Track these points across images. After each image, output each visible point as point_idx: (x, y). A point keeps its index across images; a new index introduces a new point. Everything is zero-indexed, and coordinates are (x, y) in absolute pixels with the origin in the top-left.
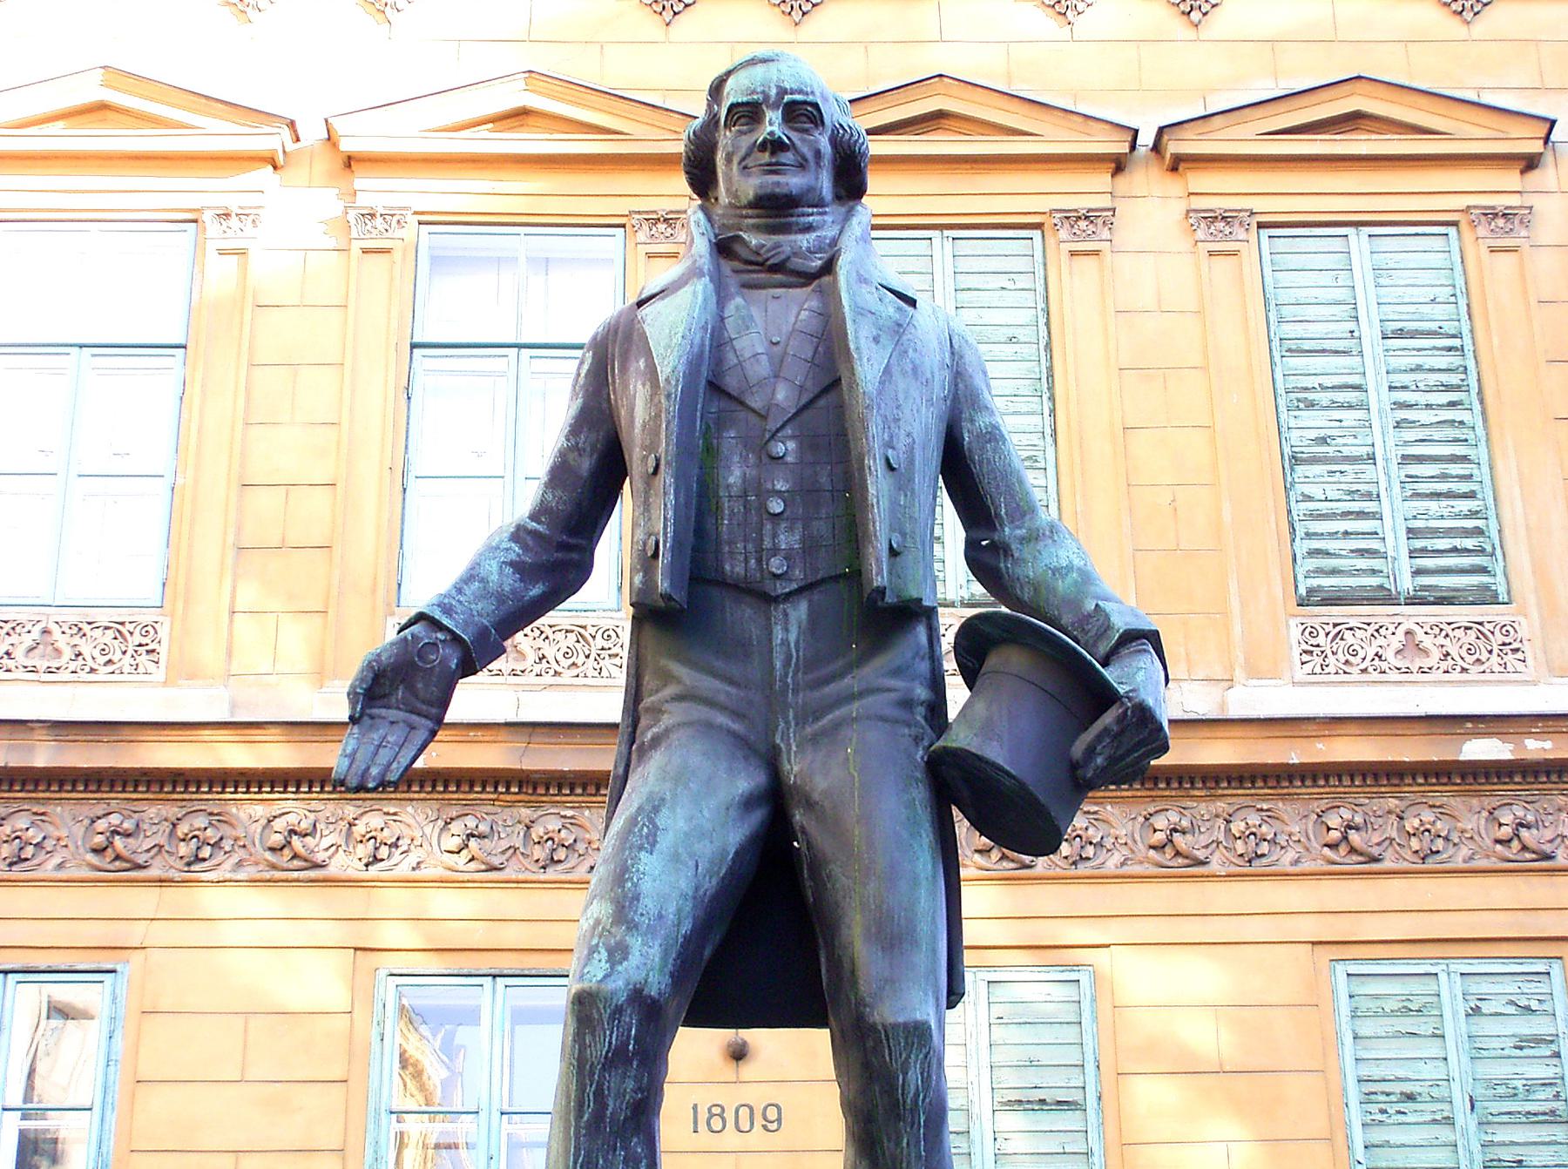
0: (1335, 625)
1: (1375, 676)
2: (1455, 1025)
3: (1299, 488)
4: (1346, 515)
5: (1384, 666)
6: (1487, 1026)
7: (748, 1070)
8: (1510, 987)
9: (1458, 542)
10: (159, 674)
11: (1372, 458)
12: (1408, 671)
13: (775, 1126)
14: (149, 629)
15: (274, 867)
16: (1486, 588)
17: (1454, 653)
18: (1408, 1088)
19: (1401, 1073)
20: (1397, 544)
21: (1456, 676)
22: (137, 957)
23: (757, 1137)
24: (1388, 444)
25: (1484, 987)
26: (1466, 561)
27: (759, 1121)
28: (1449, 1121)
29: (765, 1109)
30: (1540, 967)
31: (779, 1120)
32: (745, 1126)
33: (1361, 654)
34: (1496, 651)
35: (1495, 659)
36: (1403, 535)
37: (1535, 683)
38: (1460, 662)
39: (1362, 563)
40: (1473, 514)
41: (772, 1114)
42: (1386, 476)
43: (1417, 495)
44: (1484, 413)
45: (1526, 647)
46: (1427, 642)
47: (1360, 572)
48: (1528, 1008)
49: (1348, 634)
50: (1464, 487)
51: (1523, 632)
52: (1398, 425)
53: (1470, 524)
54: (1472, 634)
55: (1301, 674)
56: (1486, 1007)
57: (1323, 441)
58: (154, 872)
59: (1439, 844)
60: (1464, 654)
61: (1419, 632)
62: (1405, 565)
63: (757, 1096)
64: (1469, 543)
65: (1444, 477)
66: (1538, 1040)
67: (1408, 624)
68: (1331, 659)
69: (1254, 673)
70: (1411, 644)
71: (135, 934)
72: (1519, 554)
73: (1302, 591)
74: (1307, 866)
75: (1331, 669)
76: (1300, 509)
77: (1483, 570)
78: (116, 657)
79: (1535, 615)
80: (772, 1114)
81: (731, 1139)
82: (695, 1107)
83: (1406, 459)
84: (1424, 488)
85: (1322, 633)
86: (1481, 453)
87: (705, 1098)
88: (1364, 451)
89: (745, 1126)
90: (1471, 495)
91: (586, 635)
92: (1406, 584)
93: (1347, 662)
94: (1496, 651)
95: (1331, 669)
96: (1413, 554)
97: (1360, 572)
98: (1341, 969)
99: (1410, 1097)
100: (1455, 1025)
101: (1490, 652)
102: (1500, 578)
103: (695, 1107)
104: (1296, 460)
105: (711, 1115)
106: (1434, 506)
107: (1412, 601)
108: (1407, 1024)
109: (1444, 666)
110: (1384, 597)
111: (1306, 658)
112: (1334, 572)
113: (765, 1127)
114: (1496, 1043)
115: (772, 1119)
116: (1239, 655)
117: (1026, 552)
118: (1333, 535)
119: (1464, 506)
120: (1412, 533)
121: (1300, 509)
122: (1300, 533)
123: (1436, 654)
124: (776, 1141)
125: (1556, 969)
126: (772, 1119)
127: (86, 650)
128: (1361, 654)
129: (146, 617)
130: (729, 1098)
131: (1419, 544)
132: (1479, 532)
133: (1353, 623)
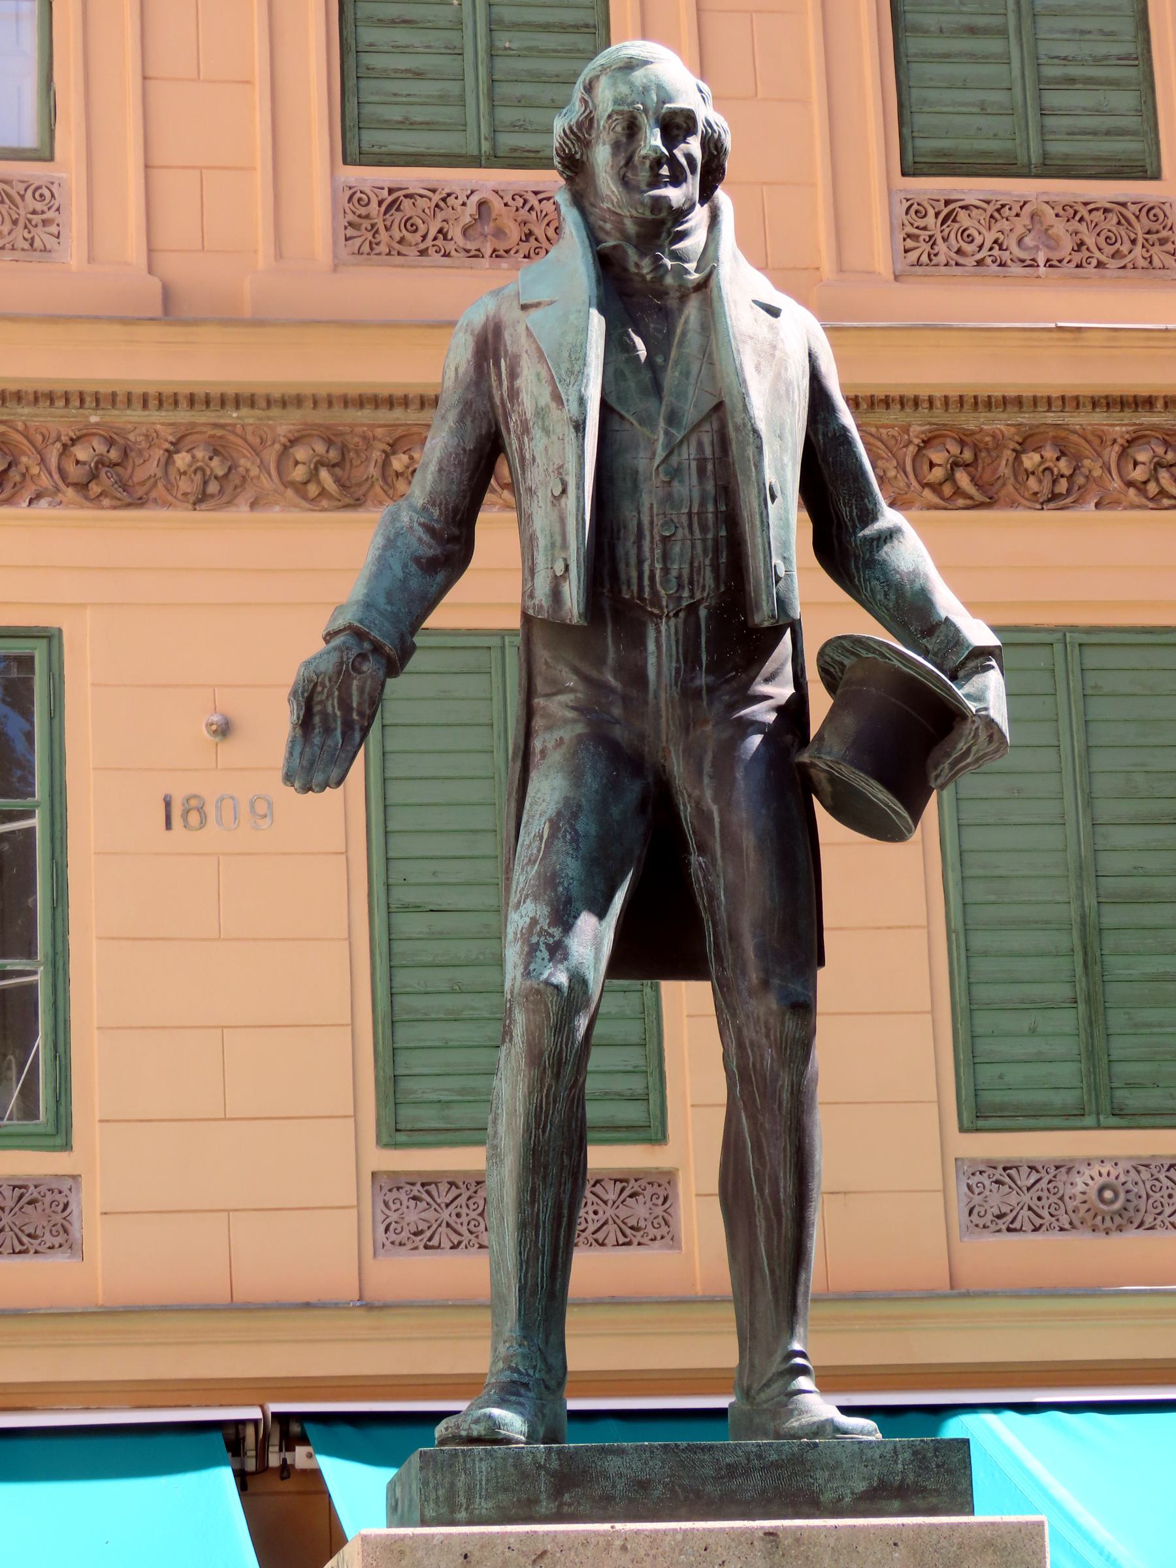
0: (947, 203)
5: (1006, 256)
17: (1090, 241)
21: (1090, 270)
33: (978, 240)
34: (1140, 241)
35: (1138, 250)
38: (1097, 254)
49: (963, 214)
60: (1103, 244)
75: (942, 259)
85: (931, 212)
91: (13, 193)
93: (959, 252)
94: (1140, 241)
95: (942, 259)
101: (1134, 242)
109: (1077, 257)
111: (910, 243)
128: (978, 240)
133: (970, 200)
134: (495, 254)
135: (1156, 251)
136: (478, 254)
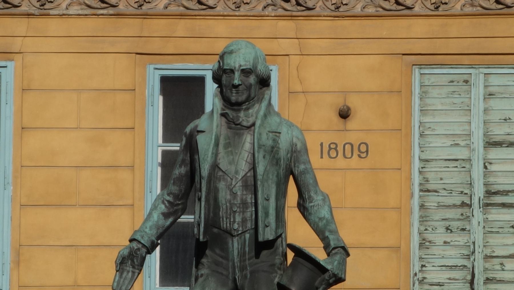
7: (352, 124)
13: (364, 155)
23: (355, 161)
27: (356, 152)
29: (360, 145)
31: (367, 151)
32: (348, 154)
41: (363, 148)
63: (354, 138)
80: (363, 148)
81: (341, 162)
82: (322, 145)
87: (327, 139)
89: (348, 154)
103: (322, 145)
105: (330, 149)
113: (359, 156)
115: (363, 151)
124: (365, 163)
126: (363, 151)
130: (340, 140)
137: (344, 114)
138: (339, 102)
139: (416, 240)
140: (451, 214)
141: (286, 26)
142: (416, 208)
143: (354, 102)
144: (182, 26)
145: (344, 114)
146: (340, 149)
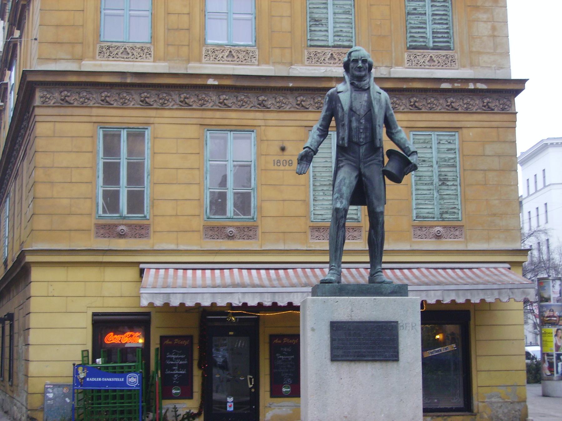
1: (423, 67)
2: (435, 146)
3: (409, 21)
4: (419, 28)
6: (442, 146)
7: (285, 153)
8: (447, 138)
9: (443, 35)
10: (152, 59)
11: (425, 14)
12: (430, 66)
14: (149, 48)
15: (181, 106)
16: (449, 46)
18: (424, 159)
19: (423, 156)
20: (429, 35)
21: (440, 67)
22: (152, 126)
24: (429, 10)
25: (441, 138)
26: (445, 40)
27: (288, 164)
28: (432, 166)
30: (453, 134)
35: (449, 63)
36: (431, 33)
37: (457, 69)
39: (421, 40)
40: (447, 28)
41: (290, 162)
42: (428, 18)
43: (435, 23)
44: (451, 3)
45: (456, 61)
46: (435, 59)
47: (420, 42)
48: (450, 143)
50: (445, 22)
51: (456, 57)
52: (432, 6)
53: (446, 31)
54: (445, 58)
55: (407, 65)
56: (442, 142)
57: (415, 9)
58: (155, 106)
59: (434, 106)
61: (433, 57)
62: (431, 40)
63: (287, 158)
64: (446, 35)
65: (441, 19)
66: (451, 149)
67: (431, 55)
68: (414, 63)
69: (397, 65)
70: (431, 60)
71: (152, 120)
72: (457, 39)
73: (408, 46)
74: (405, 110)
76: (409, 26)
77: (448, 42)
78: (142, 55)
79: (459, 52)
80: (290, 162)
81: (282, 167)
83: (433, 15)
84: (437, 21)
86: (450, 14)
87: (276, 158)
88: (424, 12)
90: (447, 24)
92: (431, 45)
96: (433, 37)
97: (420, 42)
98: (411, 133)
99: (424, 161)
100: (435, 146)
102: (452, 44)
104: (409, 14)
106: (438, 26)
107: (433, 49)
108: (424, 145)
110: (425, 48)
112: (415, 41)
114: (442, 150)
116: (394, 62)
117: (396, 135)
118: (416, 33)
119: (445, 26)
120: (433, 33)
121: (409, 26)
122: (408, 31)
123: (437, 62)
125: (457, 134)
127: (135, 53)
129: (148, 45)
130: (282, 158)
131: (435, 35)
132: (447, 33)
134: (334, 63)
135: (453, 63)
136: (331, 63)
137: (283, 149)
138: (281, 144)
139: (312, 198)
140: (325, 188)
141: (259, 115)
142: (311, 185)
143: (286, 144)
144: (218, 114)
145: (283, 149)
146: (281, 162)
